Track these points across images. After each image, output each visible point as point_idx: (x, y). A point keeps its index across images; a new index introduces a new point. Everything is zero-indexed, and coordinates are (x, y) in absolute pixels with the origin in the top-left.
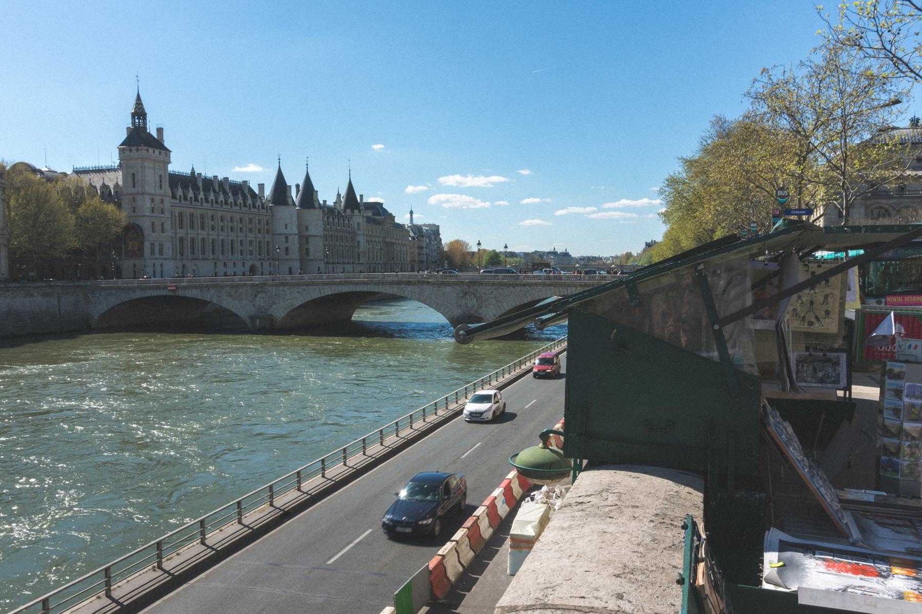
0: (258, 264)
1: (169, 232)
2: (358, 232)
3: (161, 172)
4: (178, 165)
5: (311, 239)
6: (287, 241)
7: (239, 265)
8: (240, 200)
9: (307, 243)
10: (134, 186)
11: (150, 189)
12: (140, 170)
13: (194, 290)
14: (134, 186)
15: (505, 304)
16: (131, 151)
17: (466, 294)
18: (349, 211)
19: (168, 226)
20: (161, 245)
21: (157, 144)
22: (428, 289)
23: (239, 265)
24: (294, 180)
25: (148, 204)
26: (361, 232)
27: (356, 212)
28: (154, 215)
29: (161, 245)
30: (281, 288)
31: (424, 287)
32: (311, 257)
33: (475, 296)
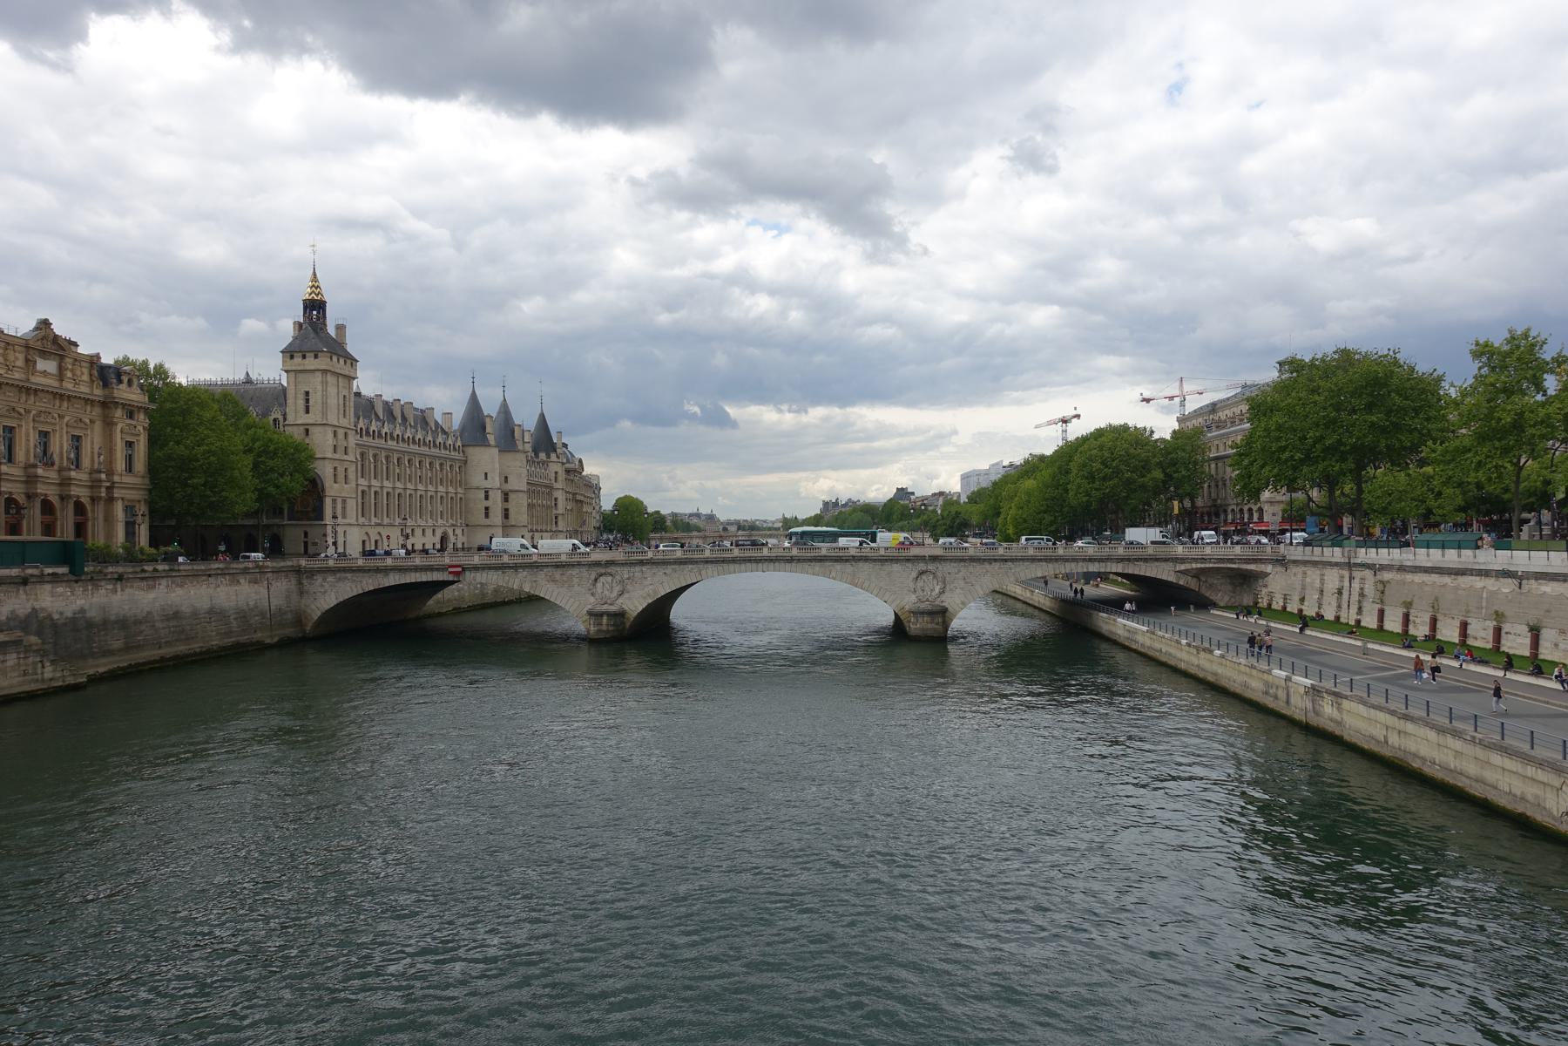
0: (450, 532)
1: (353, 485)
2: (557, 486)
3: (345, 392)
4: (367, 383)
5: (512, 496)
6: (487, 498)
7: (429, 532)
8: (430, 438)
9: (506, 500)
10: (307, 412)
11: (332, 419)
12: (319, 388)
13: (491, 573)
14: (307, 412)
15: (978, 587)
16: (304, 357)
17: (922, 573)
18: (542, 456)
19: (352, 476)
20: (344, 502)
21: (337, 349)
22: (865, 567)
23: (429, 532)
24: (490, 408)
25: (330, 440)
26: (558, 485)
27: (553, 456)
28: (337, 456)
29: (344, 502)
30: (637, 568)
31: (861, 564)
32: (512, 521)
33: (935, 576)
